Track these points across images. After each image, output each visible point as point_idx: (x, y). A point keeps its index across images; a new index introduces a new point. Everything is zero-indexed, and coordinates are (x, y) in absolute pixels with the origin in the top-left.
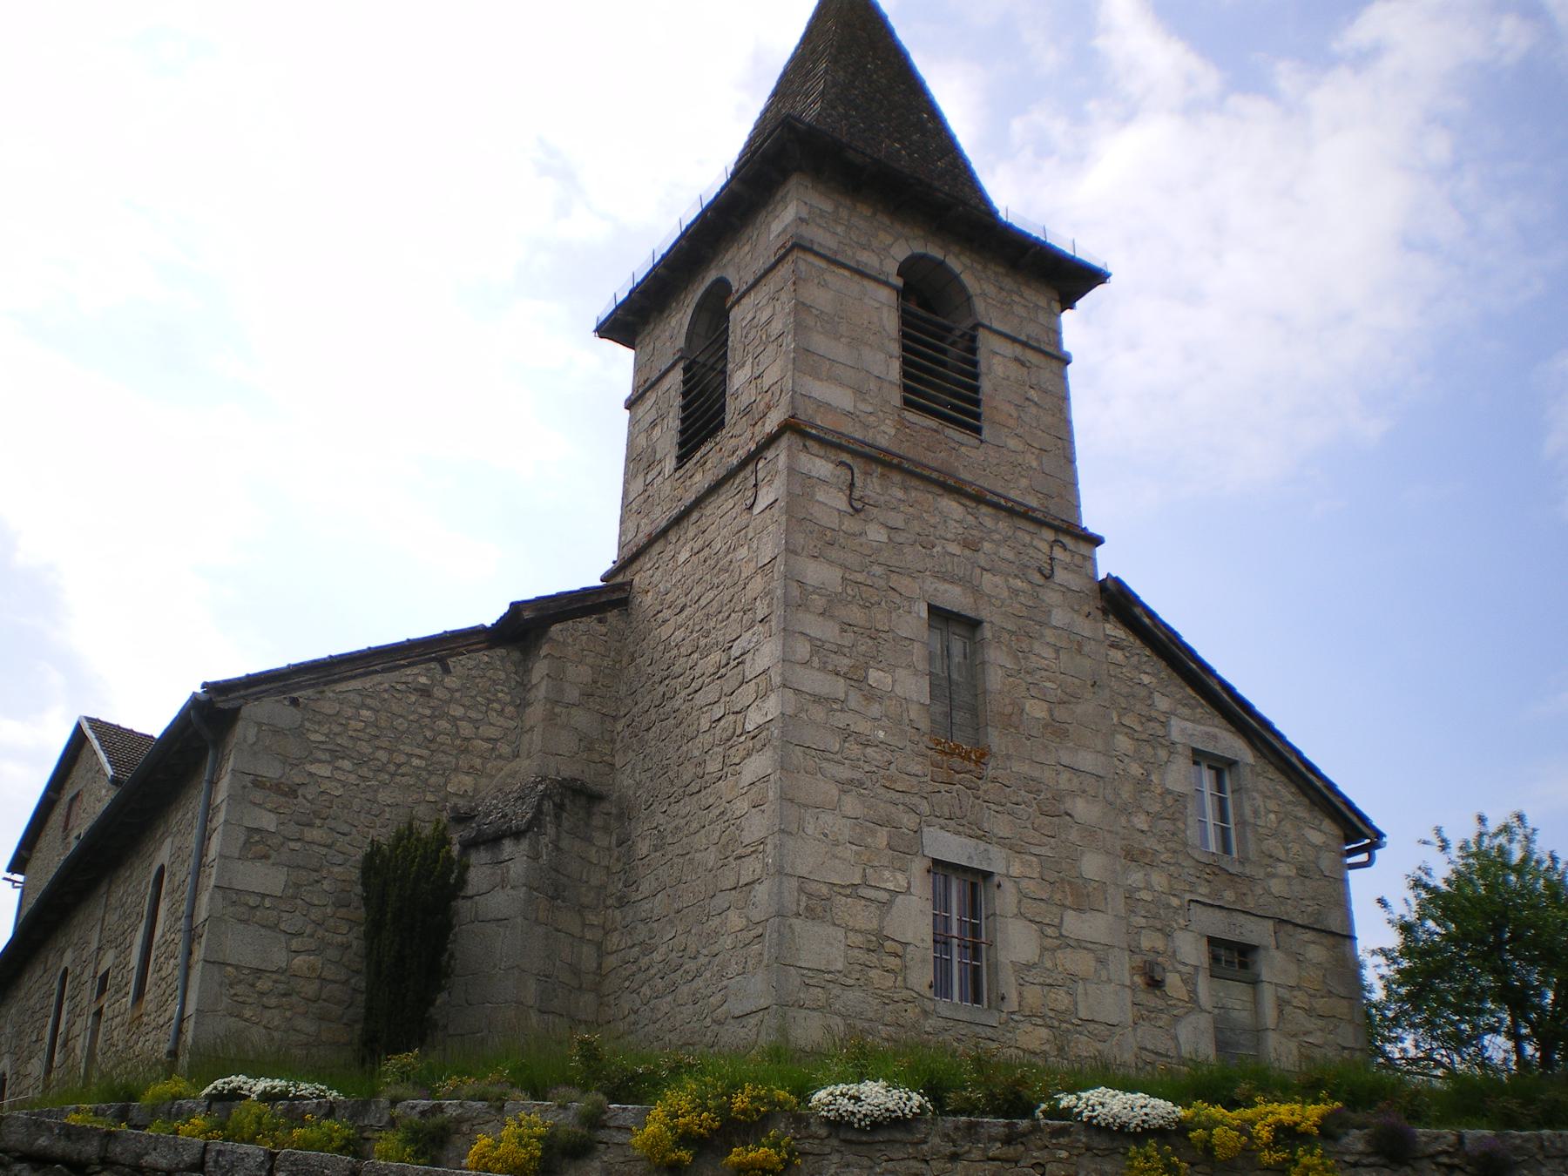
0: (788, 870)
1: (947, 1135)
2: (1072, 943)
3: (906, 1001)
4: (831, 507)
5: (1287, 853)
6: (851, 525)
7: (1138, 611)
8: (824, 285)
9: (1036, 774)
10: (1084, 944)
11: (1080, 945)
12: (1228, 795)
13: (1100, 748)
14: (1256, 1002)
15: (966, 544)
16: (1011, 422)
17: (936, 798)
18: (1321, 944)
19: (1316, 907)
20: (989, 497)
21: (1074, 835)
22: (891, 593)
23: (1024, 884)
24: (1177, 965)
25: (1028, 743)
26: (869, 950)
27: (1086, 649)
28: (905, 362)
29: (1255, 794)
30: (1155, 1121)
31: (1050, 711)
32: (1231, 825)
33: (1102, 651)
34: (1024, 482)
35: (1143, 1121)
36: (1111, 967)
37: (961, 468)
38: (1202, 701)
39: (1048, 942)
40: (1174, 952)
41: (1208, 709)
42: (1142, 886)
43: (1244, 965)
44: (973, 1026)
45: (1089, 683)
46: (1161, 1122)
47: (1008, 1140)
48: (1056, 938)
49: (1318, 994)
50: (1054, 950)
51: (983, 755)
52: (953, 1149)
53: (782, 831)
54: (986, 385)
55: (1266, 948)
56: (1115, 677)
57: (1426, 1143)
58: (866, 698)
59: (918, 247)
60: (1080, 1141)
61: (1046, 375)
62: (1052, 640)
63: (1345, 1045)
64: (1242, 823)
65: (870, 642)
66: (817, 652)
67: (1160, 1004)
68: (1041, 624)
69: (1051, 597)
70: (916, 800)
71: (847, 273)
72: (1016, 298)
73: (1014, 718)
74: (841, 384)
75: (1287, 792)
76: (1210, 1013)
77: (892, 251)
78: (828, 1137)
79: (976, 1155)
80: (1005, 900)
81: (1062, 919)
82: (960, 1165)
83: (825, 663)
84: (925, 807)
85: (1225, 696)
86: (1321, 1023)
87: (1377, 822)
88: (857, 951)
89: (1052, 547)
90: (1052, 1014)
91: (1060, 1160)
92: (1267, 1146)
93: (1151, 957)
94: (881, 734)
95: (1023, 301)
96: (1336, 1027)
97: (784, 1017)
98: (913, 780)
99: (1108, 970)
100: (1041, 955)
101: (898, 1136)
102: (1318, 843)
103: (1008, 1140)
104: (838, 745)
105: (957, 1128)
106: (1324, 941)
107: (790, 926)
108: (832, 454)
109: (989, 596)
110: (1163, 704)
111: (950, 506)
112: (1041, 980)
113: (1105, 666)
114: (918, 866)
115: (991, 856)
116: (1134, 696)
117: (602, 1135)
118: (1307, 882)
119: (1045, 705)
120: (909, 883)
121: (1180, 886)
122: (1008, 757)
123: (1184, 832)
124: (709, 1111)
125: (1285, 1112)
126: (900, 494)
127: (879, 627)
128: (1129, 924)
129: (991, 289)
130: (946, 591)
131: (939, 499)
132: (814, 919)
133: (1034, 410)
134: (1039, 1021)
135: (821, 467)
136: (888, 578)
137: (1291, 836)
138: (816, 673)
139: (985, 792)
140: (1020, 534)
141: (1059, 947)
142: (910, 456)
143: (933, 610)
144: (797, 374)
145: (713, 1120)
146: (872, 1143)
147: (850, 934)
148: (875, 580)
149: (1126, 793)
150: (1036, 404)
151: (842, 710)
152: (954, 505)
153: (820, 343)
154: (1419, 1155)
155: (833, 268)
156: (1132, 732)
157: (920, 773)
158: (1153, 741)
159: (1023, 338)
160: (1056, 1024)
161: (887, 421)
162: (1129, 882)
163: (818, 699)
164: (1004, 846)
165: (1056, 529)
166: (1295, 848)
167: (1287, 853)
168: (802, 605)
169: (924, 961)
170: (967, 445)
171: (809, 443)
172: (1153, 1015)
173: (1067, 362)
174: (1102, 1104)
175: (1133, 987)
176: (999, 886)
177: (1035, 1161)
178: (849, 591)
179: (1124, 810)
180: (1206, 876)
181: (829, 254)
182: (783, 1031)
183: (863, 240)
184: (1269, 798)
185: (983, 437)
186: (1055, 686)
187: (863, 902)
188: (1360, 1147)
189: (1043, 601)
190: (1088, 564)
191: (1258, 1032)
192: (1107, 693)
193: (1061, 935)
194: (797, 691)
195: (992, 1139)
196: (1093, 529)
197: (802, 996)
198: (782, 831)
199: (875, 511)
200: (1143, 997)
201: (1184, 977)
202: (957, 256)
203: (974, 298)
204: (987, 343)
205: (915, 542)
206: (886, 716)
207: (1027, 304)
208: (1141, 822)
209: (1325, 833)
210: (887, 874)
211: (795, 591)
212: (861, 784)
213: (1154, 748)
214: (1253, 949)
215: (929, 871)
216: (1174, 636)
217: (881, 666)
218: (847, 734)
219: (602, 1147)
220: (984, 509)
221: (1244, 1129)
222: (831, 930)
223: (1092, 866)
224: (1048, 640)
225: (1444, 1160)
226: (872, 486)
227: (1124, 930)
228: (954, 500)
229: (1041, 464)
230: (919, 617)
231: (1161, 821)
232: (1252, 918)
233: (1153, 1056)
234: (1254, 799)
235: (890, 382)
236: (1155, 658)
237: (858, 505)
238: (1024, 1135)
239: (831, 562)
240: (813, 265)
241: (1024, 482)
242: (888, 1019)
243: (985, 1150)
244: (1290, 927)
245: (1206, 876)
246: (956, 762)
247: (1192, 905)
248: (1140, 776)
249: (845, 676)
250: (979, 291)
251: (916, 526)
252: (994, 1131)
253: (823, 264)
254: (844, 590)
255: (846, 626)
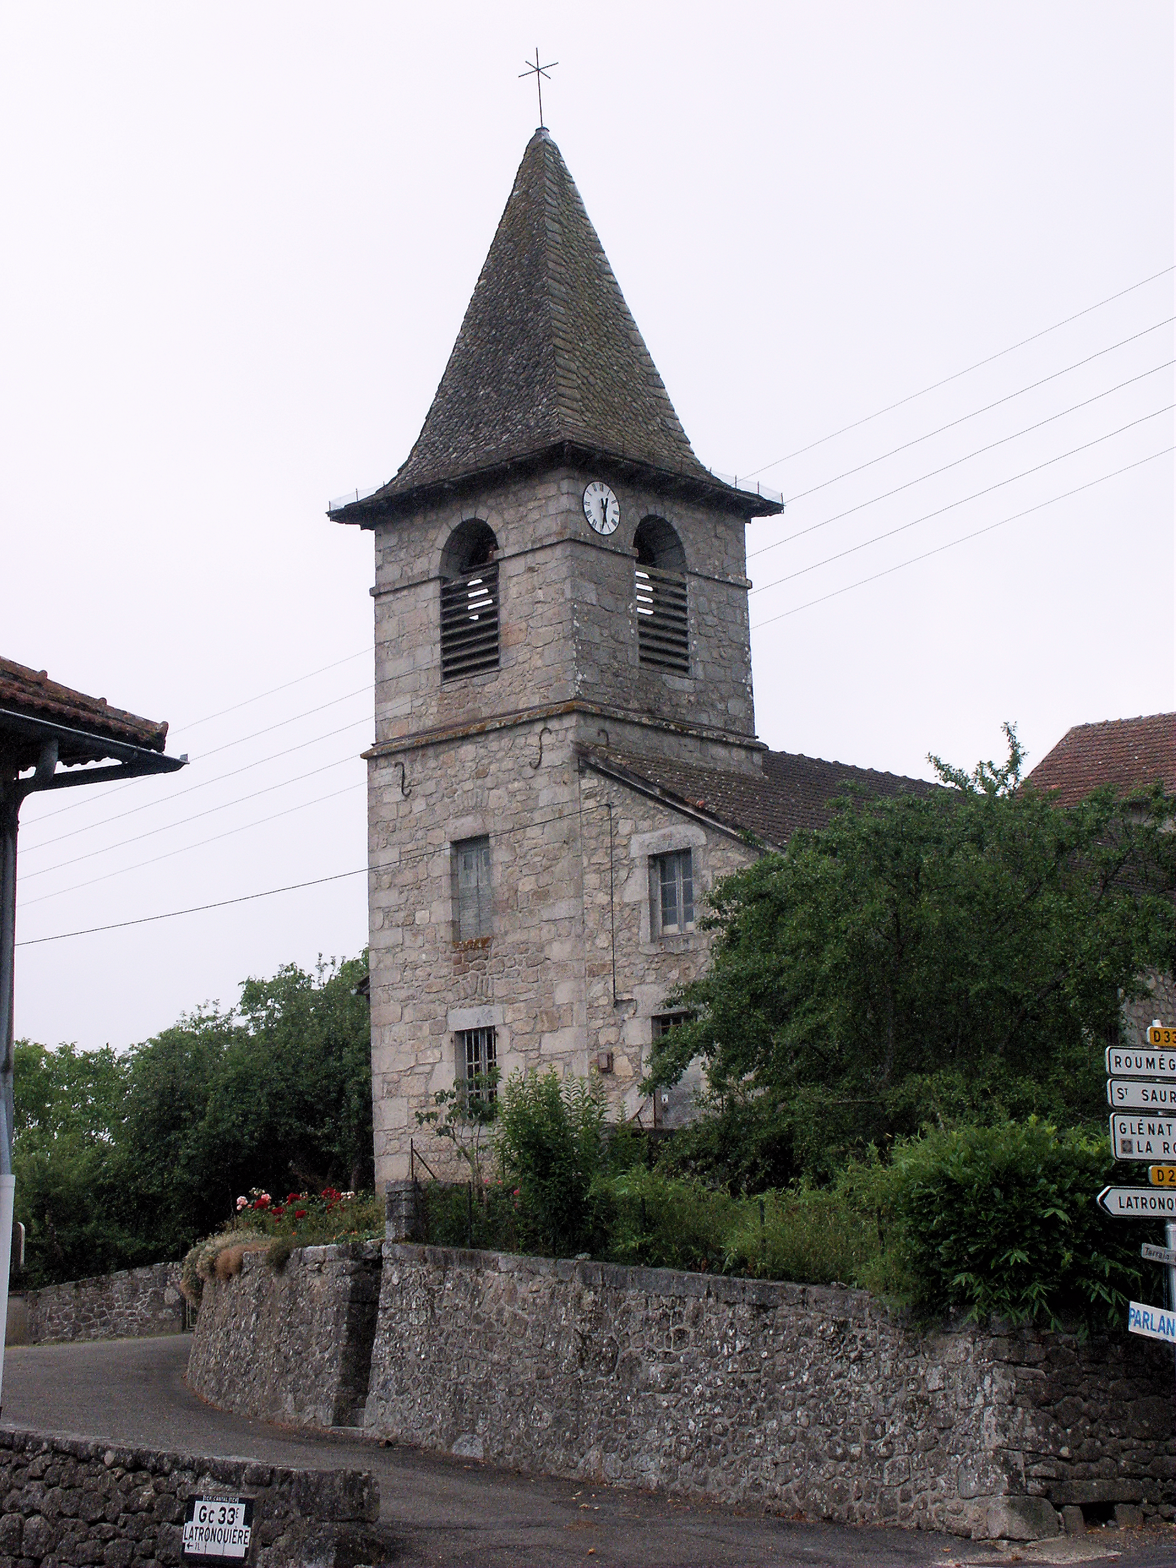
21: (552, 975)
25: (520, 915)
48: (537, 1058)
59: (455, 523)
69: (541, 781)
84: (450, 996)
111: (468, 751)
122: (506, 933)
155: (398, 595)
193: (540, 1055)
212: (413, 997)
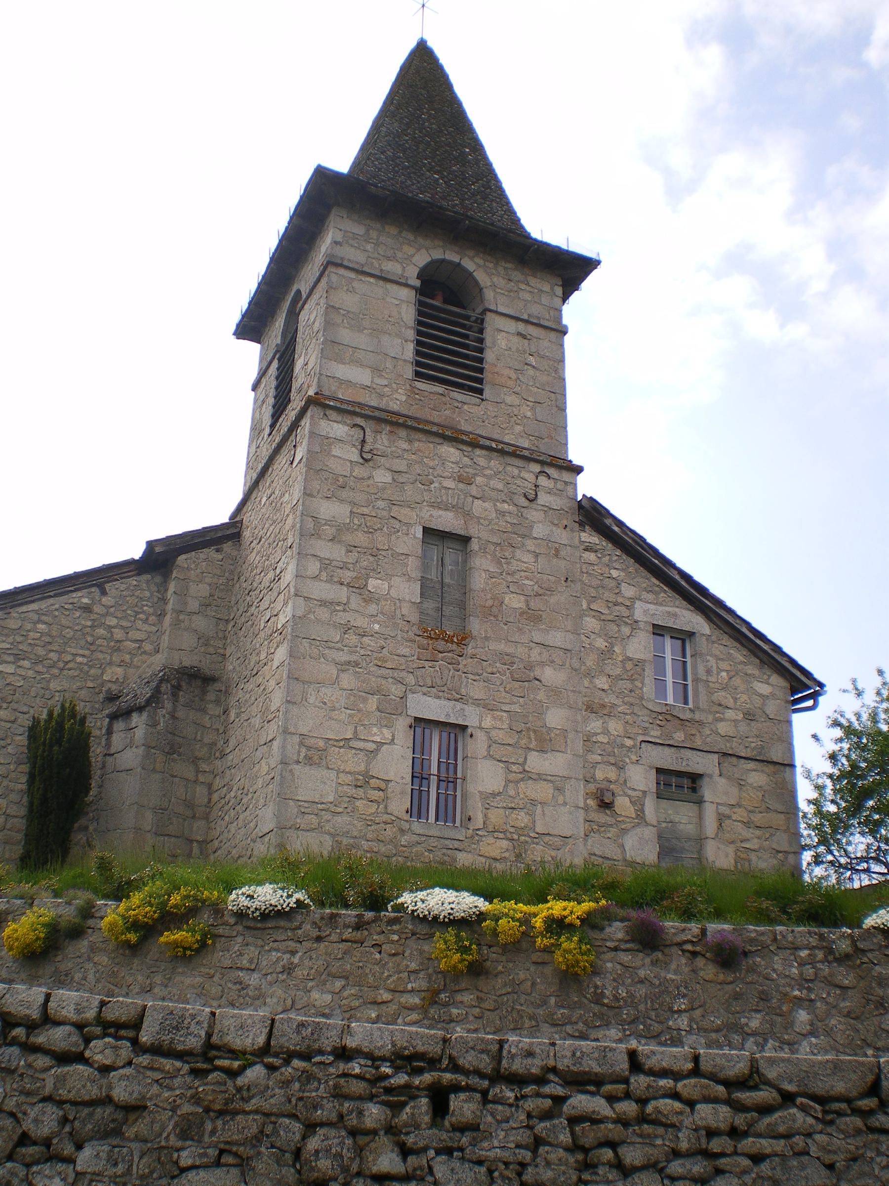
0: (292, 730)
1: (315, 923)
2: (534, 777)
3: (386, 823)
4: (344, 460)
5: (735, 702)
6: (358, 471)
7: (608, 521)
8: (353, 291)
9: (510, 650)
10: (544, 777)
11: (541, 777)
12: (688, 659)
13: (569, 628)
14: (700, 817)
15: (461, 480)
16: (511, 383)
17: (419, 673)
18: (763, 771)
19: (760, 743)
20: (482, 442)
21: (541, 695)
22: (392, 521)
23: (494, 733)
24: (626, 790)
25: (505, 627)
26: (356, 786)
27: (563, 553)
28: (419, 343)
29: (708, 658)
30: (457, 914)
31: (527, 602)
32: (689, 682)
33: (577, 554)
34: (518, 428)
35: (449, 914)
36: (567, 793)
37: (462, 422)
38: (665, 588)
39: (512, 776)
40: (625, 781)
41: (671, 593)
42: (599, 731)
43: (694, 790)
44: (443, 840)
45: (563, 579)
46: (462, 914)
47: (358, 927)
48: (520, 773)
49: (757, 810)
50: (518, 782)
51: (464, 639)
52: (318, 933)
53: (288, 702)
54: (489, 356)
55: (710, 776)
56: (587, 573)
57: (674, 934)
58: (365, 600)
59: (438, 255)
60: (407, 928)
61: (545, 341)
62: (532, 548)
63: (779, 849)
64: (696, 680)
65: (372, 559)
66: (326, 568)
67: (609, 820)
68: (523, 536)
69: (534, 515)
70: (403, 674)
71: (372, 280)
72: (523, 287)
73: (494, 609)
74: (362, 366)
75: (738, 655)
76: (654, 826)
77: (414, 260)
78: (235, 924)
79: (334, 937)
80: (478, 745)
81: (526, 759)
82: (322, 945)
83: (332, 576)
84: (411, 679)
85: (683, 583)
86: (758, 832)
87: (817, 675)
88: (346, 787)
89: (537, 477)
90: (512, 830)
91: (393, 942)
92: (541, 933)
93: (604, 785)
94: (377, 627)
95: (528, 288)
96: (772, 835)
97: (282, 836)
98: (402, 660)
99: (564, 796)
100: (506, 786)
101: (282, 923)
102: (765, 693)
103: (358, 927)
104: (339, 637)
105: (322, 918)
106: (766, 769)
107: (291, 771)
108: (349, 420)
109: (479, 518)
110: (628, 591)
111: (450, 452)
112: (505, 805)
113: (578, 566)
114: (402, 724)
115: (466, 714)
116: (603, 587)
117: (91, 922)
118: (753, 724)
119: (522, 598)
120: (393, 736)
121: (633, 730)
122: (487, 638)
123: (641, 689)
124: (152, 907)
125: (557, 908)
126: (405, 446)
127: (379, 547)
128: (586, 761)
129: (499, 281)
130: (440, 516)
131: (439, 447)
132: (311, 765)
133: (531, 372)
134: (501, 835)
135: (338, 429)
136: (390, 511)
137: (741, 689)
138: (323, 584)
139: (465, 665)
140: (509, 468)
141: (522, 780)
142: (418, 416)
143: (426, 531)
144: (324, 361)
145: (155, 912)
146: (265, 929)
147: (341, 775)
148: (379, 511)
149: (591, 661)
150: (534, 367)
151: (344, 610)
152: (452, 450)
153: (345, 335)
154: (668, 943)
155: (360, 277)
156: (598, 614)
157: (407, 654)
158: (618, 620)
159: (525, 317)
160: (516, 837)
161: (400, 391)
162: (588, 729)
163: (323, 603)
164: (478, 705)
165: (542, 463)
166: (744, 697)
167: (735, 702)
168: (316, 534)
169: (403, 793)
170: (469, 404)
171: (329, 412)
172: (603, 829)
173: (565, 333)
174: (423, 901)
175: (586, 809)
176: (471, 736)
177: (374, 942)
178: (356, 521)
179: (589, 675)
180: (658, 722)
181: (356, 267)
182: (281, 846)
183: (389, 253)
184: (722, 660)
185: (484, 397)
186: (532, 583)
187: (354, 751)
188: (620, 935)
189: (527, 519)
190: (569, 489)
191: (700, 840)
192: (578, 586)
193: (524, 770)
194: (307, 599)
195: (346, 926)
196: (576, 461)
197: (298, 821)
198: (288, 702)
199: (383, 459)
200: (595, 816)
201: (633, 800)
202: (471, 258)
203: (485, 290)
204: (492, 322)
205: (416, 480)
206: (382, 613)
207: (532, 290)
208: (602, 682)
209: (772, 685)
210: (375, 730)
211: (310, 525)
212: (357, 664)
213: (618, 626)
214: (699, 776)
215: (410, 727)
216: (640, 540)
217: (379, 576)
218: (347, 629)
219: (90, 931)
220: (478, 452)
221: (526, 921)
222: (325, 772)
223: (555, 718)
224: (529, 548)
225: (689, 947)
226: (381, 441)
227: (581, 766)
228: (453, 446)
229: (535, 414)
230: (415, 537)
231: (620, 682)
232: (699, 753)
233: (601, 860)
234: (708, 661)
235: (405, 361)
236: (624, 557)
237: (367, 456)
238: (368, 923)
239: (342, 501)
240: (343, 276)
241: (518, 428)
242: (370, 836)
243: (341, 934)
244: (734, 760)
245: (658, 722)
246: (441, 644)
247: (643, 745)
248: (603, 648)
249: (349, 585)
250: (489, 284)
251: (417, 469)
252: (347, 920)
253: (352, 275)
254: (352, 521)
255: (351, 548)
